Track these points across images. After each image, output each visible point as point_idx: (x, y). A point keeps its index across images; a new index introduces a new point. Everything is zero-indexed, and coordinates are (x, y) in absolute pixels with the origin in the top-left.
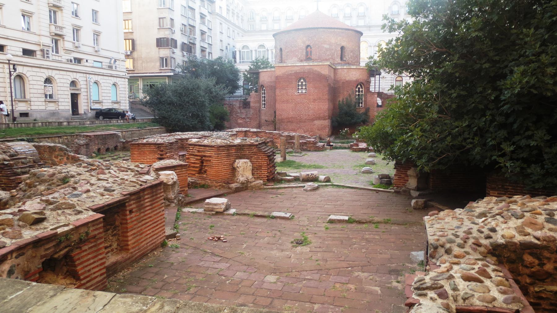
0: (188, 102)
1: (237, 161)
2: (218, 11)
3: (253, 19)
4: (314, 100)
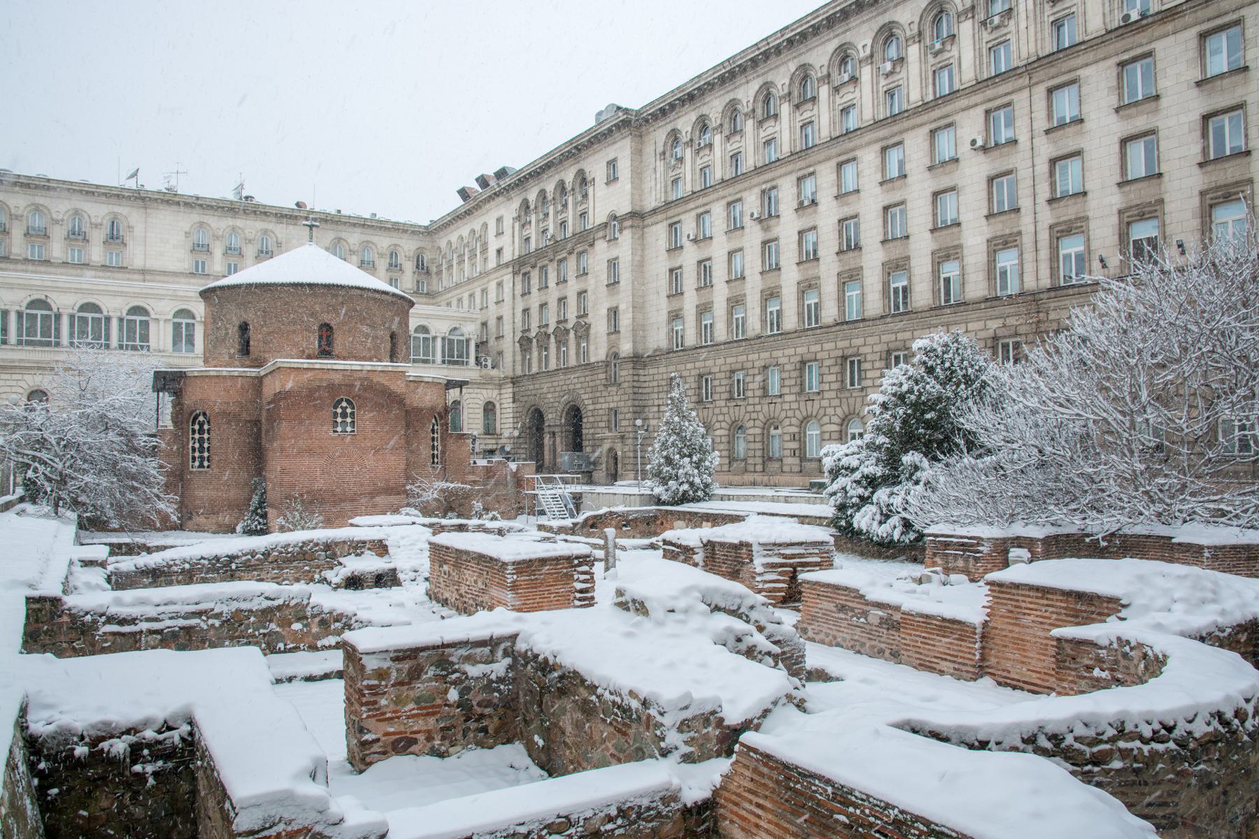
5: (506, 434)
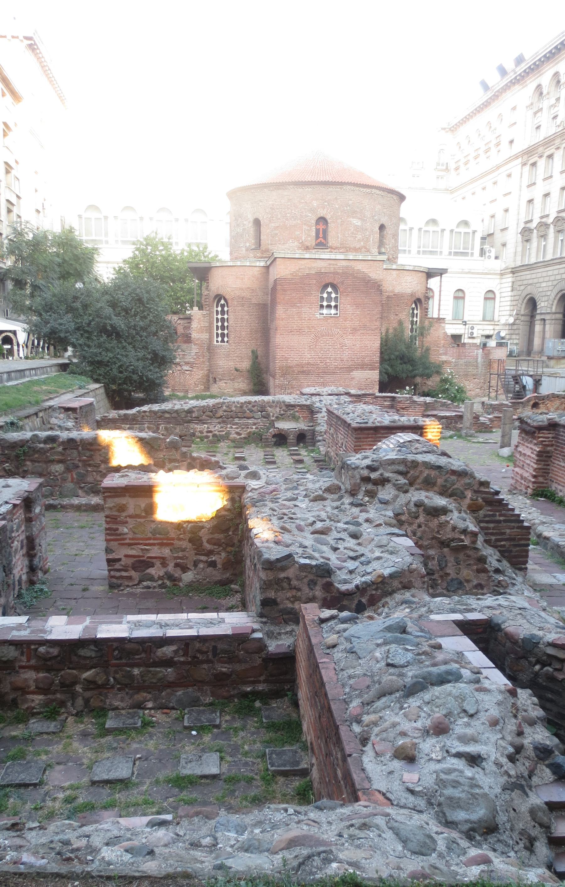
0: (144, 329)
4: (354, 330)
5: (503, 321)
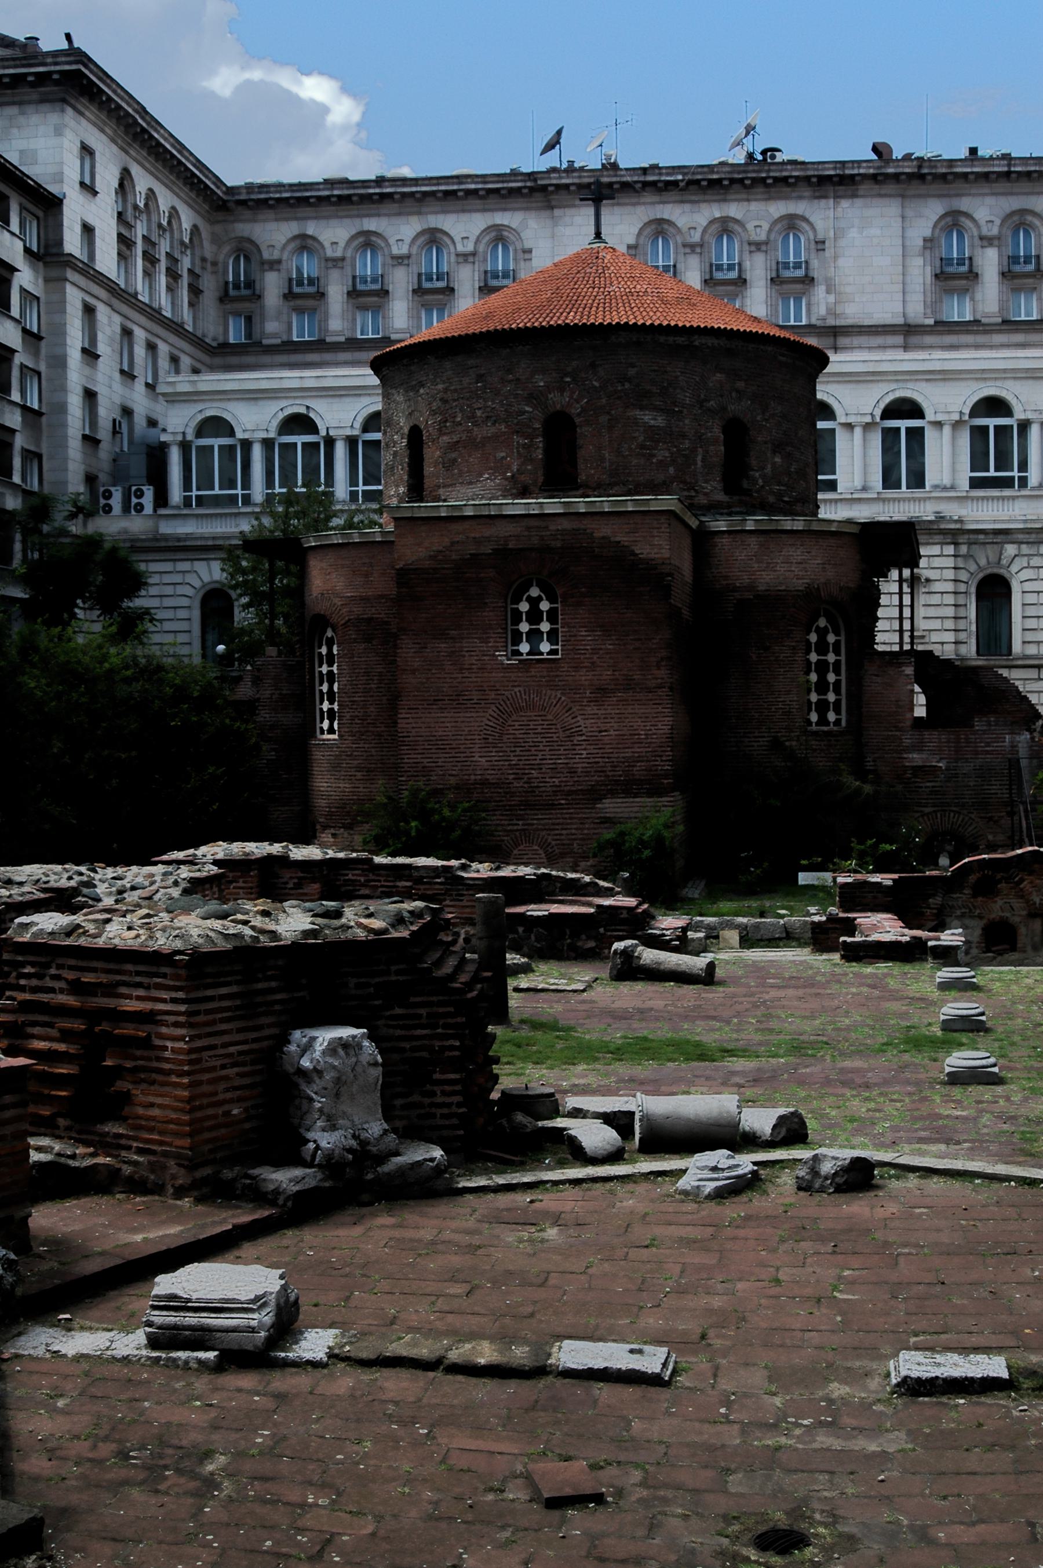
1: (297, 1034)
2: (72, 243)
3: (250, 284)
4: (601, 692)
